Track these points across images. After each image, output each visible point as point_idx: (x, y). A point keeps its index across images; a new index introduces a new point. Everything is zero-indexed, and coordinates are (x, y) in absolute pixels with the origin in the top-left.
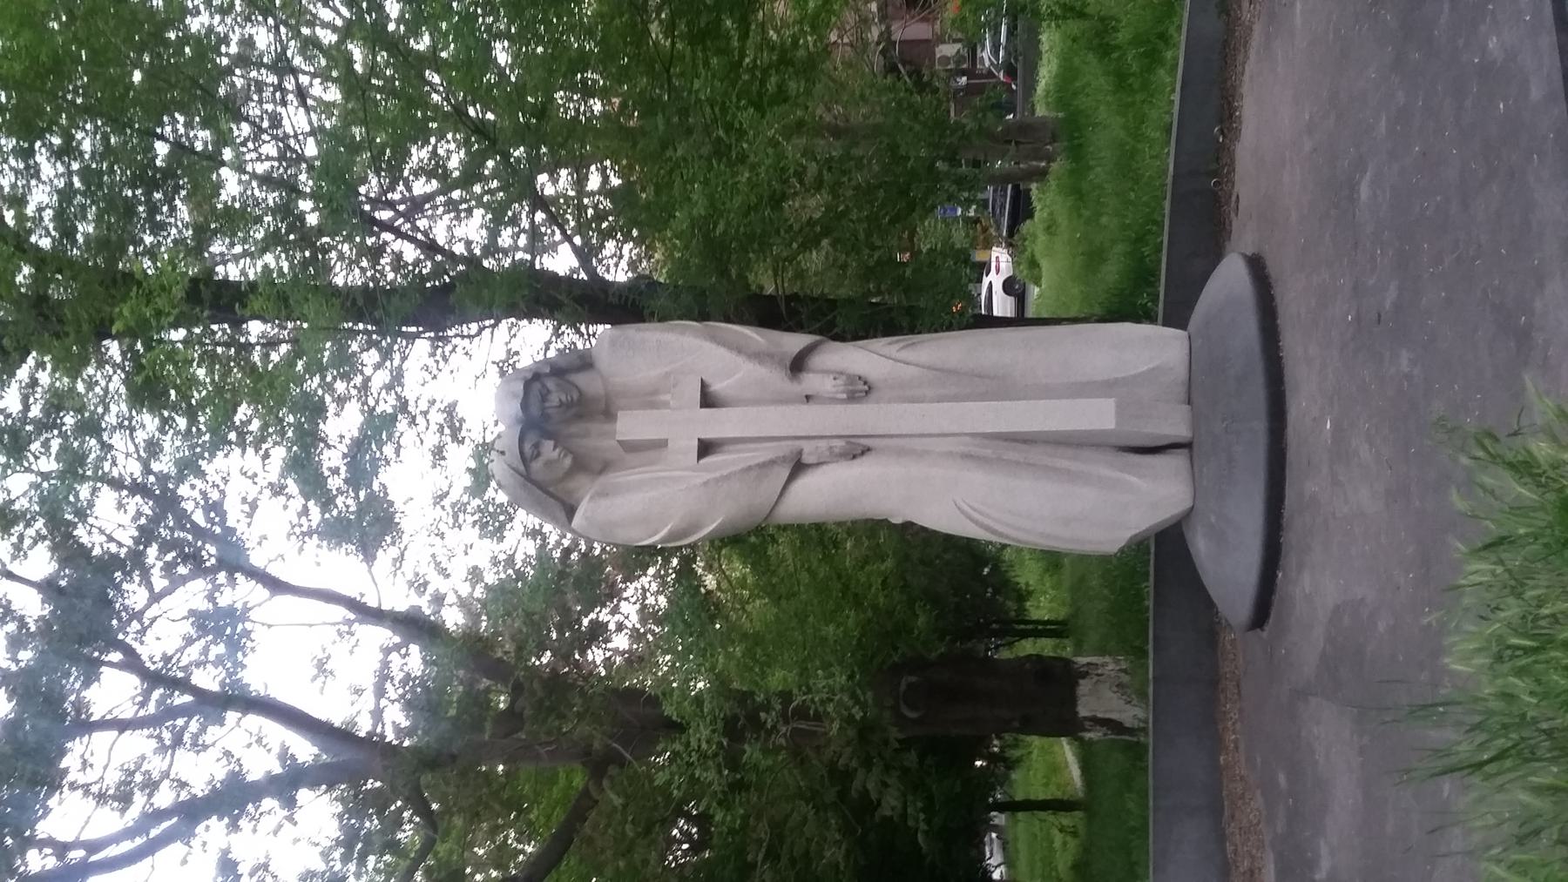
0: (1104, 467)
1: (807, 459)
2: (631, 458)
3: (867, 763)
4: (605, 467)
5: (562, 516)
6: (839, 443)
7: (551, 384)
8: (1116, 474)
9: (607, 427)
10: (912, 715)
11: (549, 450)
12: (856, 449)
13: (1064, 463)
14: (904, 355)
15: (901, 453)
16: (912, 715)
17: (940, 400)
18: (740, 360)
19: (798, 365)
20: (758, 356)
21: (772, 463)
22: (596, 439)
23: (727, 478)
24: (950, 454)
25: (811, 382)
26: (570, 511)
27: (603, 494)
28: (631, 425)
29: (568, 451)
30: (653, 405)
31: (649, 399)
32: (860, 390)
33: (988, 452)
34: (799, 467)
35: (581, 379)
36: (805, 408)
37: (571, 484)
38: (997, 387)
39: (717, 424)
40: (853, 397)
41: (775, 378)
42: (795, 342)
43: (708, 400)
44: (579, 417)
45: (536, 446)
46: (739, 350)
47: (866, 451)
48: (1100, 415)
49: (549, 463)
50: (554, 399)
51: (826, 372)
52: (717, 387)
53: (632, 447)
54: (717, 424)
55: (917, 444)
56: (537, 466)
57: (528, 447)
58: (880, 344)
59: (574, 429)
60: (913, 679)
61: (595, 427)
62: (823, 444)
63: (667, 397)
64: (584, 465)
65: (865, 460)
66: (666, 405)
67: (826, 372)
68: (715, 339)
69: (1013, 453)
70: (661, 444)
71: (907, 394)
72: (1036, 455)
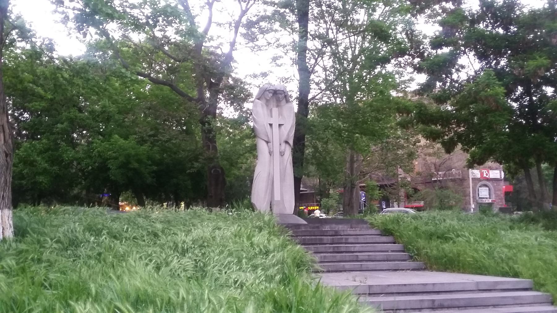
0: (267, 199)
1: (269, 144)
2: (269, 111)
3: (205, 159)
4: (267, 106)
5: (258, 98)
6: (272, 150)
7: (283, 95)
8: (266, 201)
9: (275, 106)
10: (212, 171)
11: (271, 95)
12: (271, 153)
13: (268, 192)
14: (288, 162)
15: (270, 161)
16: (212, 171)
17: (280, 169)
18: (288, 131)
19: (287, 142)
20: (288, 135)
21: (268, 138)
22: (273, 103)
23: (265, 129)
24: (270, 171)
25: (284, 145)
26: (259, 99)
27: (262, 105)
28: (275, 110)
29: (270, 99)
30: (279, 115)
31: (280, 114)
32: (282, 154)
33: (270, 177)
34: (267, 142)
35: (284, 101)
36: (279, 144)
37: (264, 99)
38: (282, 179)
39: (275, 127)
40: (280, 152)
41: (284, 138)
42: (291, 142)
43: (280, 125)
44: (277, 100)
45: (271, 92)
46: (289, 131)
47: (270, 155)
48: (277, 197)
49: (268, 95)
50: (280, 96)
51: (285, 148)
52: (283, 127)
53: (271, 111)
54: (275, 127)
55: (272, 165)
56: (267, 92)
57: (271, 91)
58: (291, 158)
59: (275, 100)
60: (220, 172)
61: (275, 104)
62: (272, 147)
63: (281, 118)
64: (267, 101)
65: (269, 155)
66: (279, 117)
67: (285, 148)
68: (292, 126)
69: (270, 183)
70: (272, 117)
71: (281, 163)
72: (270, 186)
